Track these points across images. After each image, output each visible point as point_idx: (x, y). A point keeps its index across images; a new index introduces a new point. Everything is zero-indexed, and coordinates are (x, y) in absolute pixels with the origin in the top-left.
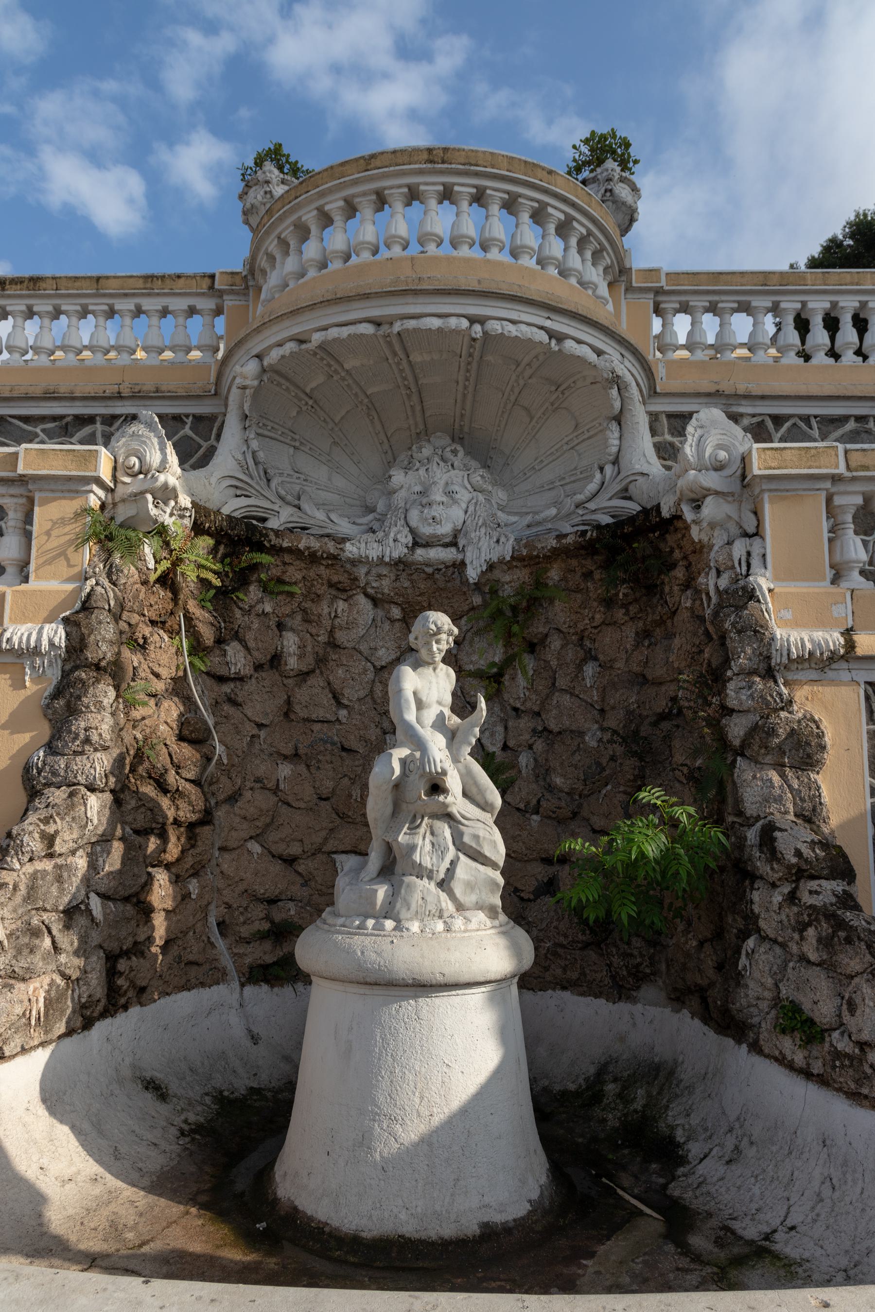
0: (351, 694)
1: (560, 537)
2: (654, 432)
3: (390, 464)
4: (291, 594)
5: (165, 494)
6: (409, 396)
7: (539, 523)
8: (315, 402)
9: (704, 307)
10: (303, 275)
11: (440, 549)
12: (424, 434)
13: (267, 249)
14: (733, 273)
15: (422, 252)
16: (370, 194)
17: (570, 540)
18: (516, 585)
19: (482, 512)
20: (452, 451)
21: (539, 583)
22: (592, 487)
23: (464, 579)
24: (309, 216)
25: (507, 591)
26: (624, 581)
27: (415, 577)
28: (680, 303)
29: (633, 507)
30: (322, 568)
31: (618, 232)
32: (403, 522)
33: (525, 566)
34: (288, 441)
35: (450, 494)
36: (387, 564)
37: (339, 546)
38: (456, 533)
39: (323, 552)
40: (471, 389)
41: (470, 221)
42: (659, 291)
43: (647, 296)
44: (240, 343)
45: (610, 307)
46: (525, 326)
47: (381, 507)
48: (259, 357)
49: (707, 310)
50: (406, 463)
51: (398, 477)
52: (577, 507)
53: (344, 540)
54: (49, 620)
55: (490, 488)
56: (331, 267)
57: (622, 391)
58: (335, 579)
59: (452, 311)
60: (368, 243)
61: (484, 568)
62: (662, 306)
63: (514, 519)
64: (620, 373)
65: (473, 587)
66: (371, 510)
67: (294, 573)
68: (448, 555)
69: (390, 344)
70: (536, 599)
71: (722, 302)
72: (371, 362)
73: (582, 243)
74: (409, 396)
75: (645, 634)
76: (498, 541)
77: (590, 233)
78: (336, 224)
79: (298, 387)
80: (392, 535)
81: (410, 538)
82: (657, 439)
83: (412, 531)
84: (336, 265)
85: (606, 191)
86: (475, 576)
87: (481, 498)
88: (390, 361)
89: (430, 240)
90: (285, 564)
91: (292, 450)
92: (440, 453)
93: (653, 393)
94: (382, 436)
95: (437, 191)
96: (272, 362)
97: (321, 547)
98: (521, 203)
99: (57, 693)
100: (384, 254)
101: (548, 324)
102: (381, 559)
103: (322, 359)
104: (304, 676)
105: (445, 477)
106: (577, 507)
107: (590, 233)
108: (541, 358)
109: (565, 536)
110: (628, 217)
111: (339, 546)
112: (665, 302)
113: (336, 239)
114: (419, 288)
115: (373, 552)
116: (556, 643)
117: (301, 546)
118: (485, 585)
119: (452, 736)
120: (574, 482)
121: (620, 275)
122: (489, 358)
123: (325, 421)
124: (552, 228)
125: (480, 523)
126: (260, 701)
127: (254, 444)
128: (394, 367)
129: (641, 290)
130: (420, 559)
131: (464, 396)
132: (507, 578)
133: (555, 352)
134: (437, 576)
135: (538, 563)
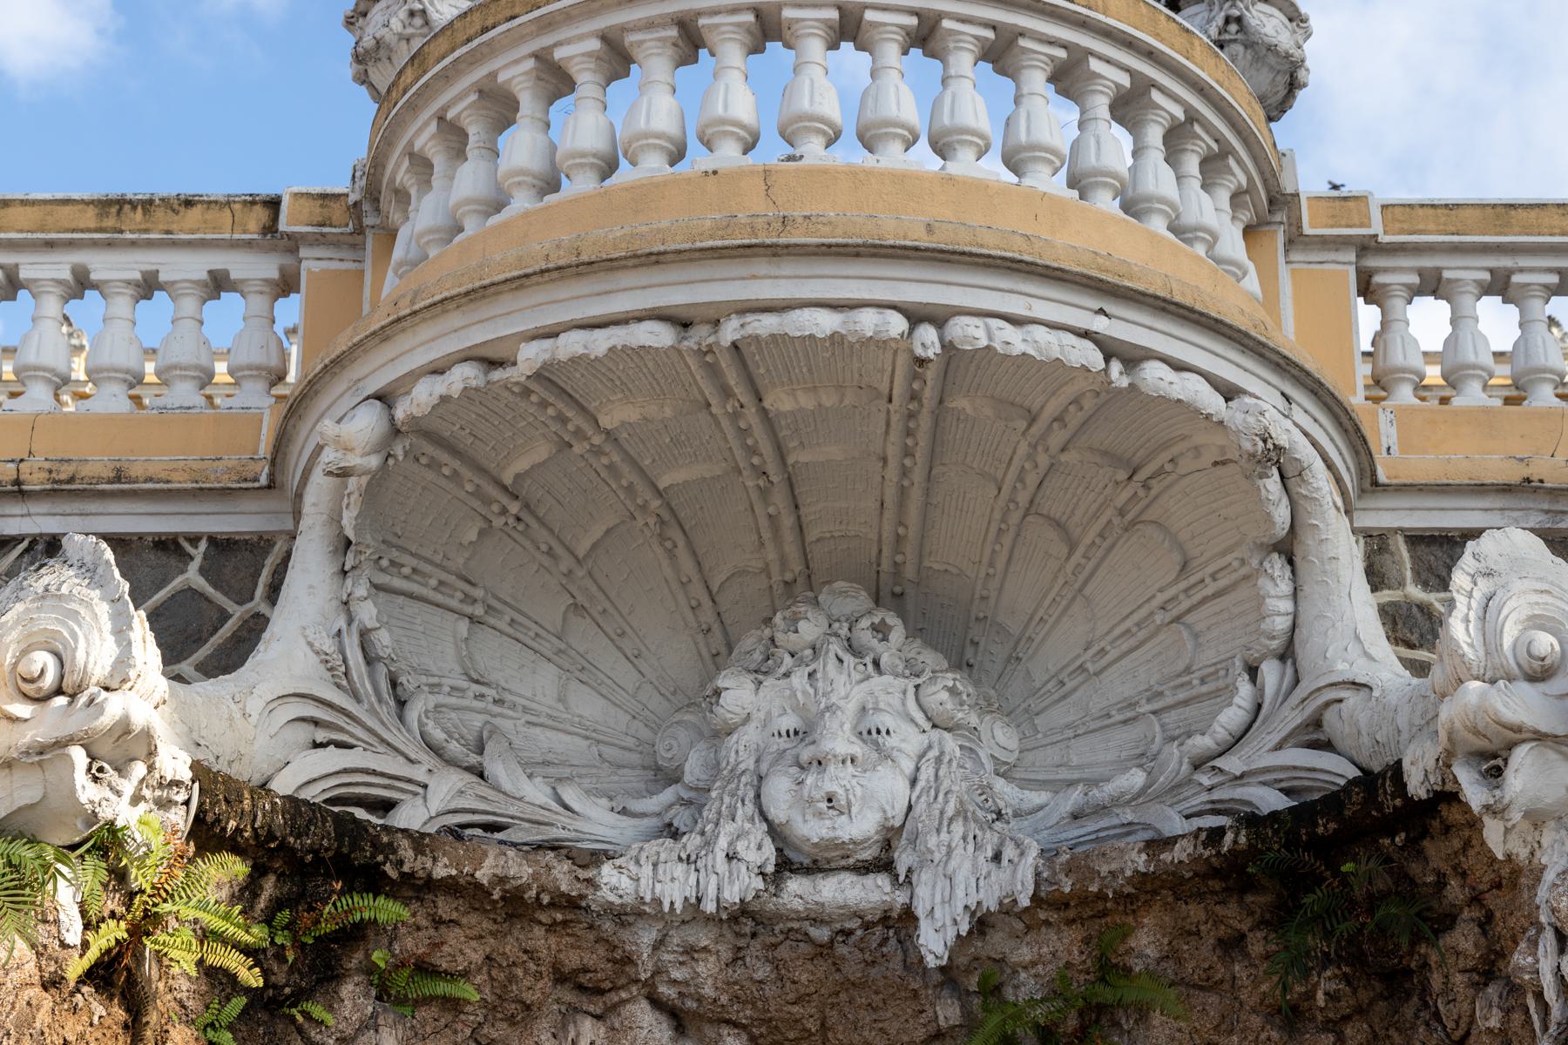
1: (1158, 844)
2: (1376, 578)
3: (718, 661)
4: (453, 1005)
6: (764, 493)
7: (1101, 809)
8: (527, 506)
9: (1478, 283)
10: (498, 206)
11: (848, 878)
12: (803, 585)
13: (411, 143)
14: (1542, 206)
15: (791, 158)
16: (664, 26)
17: (1181, 852)
18: (1048, 970)
19: (956, 783)
20: (875, 628)
21: (1108, 968)
22: (1232, 717)
23: (912, 958)
24: (516, 72)
26: (1326, 961)
27: (783, 952)
28: (1421, 272)
29: (1337, 769)
30: (539, 931)
31: (1261, 113)
32: (750, 808)
33: (1070, 922)
34: (454, 603)
35: (871, 735)
36: (709, 919)
37: (583, 874)
38: (889, 838)
39: (542, 889)
40: (918, 475)
41: (905, 89)
42: (1367, 246)
43: (1341, 257)
44: (336, 365)
45: (1252, 283)
47: (693, 769)
48: (384, 398)
49: (1487, 290)
50: (758, 656)
51: (738, 693)
52: (1197, 766)
53: (596, 858)
55: (974, 720)
56: (569, 189)
57: (1291, 483)
58: (572, 960)
59: (866, 296)
60: (659, 136)
61: (964, 928)
62: (1378, 279)
63: (1037, 798)
64: (1283, 441)
65: (938, 977)
66: (668, 776)
67: (463, 947)
68: (870, 893)
69: (713, 371)
70: (1101, 1009)
71: (1521, 270)
72: (668, 412)
73: (1175, 139)
74: (764, 493)
76: (997, 857)
77: (1192, 117)
78: (582, 91)
79: (481, 470)
80: (723, 843)
81: (769, 851)
82: (1387, 596)
83: (774, 831)
84: (580, 185)
85: (1228, 20)
86: (939, 949)
87: (951, 744)
88: (714, 410)
89: (809, 130)
90: (438, 922)
91: (463, 626)
92: (844, 632)
93: (1371, 484)
94: (698, 590)
95: (825, 22)
96: (417, 412)
97: (535, 877)
98: (1025, 50)
100: (698, 160)
101: (1100, 325)
102: (694, 906)
103: (544, 404)
105: (858, 694)
106: (1197, 766)
107: (1192, 117)
108: (1089, 404)
109: (1170, 842)
110: (1283, 79)
111: (583, 874)
112: (1386, 270)
113: (583, 124)
114: (783, 240)
115: (675, 888)
117: (483, 875)
118: (968, 971)
120: (1186, 703)
121: (1270, 210)
122: (960, 403)
123: (550, 552)
124: (1101, 105)
125: (950, 811)
127: (367, 613)
128: (725, 423)
129: (1325, 243)
130: (797, 905)
131: (903, 492)
132: (1025, 953)
133: (1120, 391)
134: (842, 950)
135: (1104, 913)
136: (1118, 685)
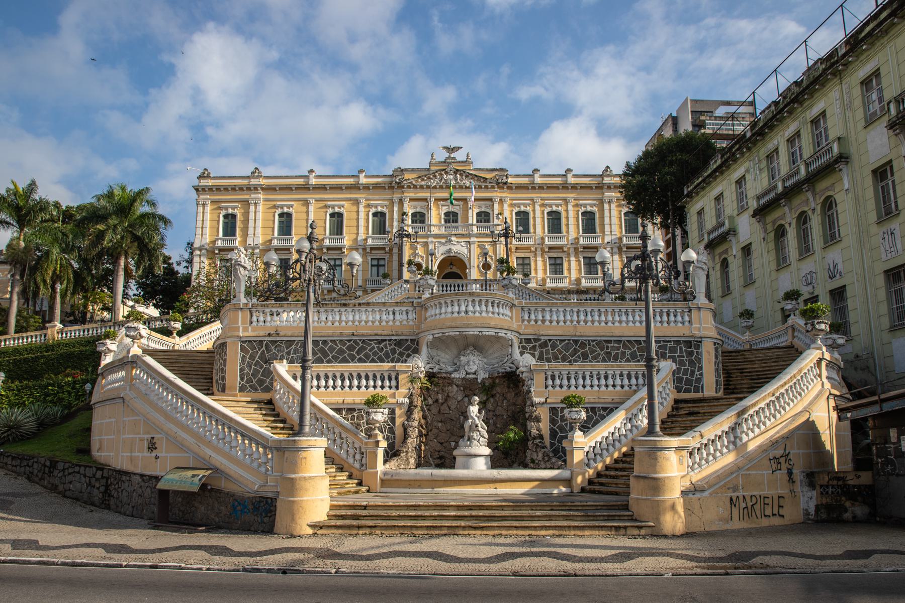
0: (453, 407)
5: (422, 372)
54: (405, 397)
104: (442, 404)
126: (434, 410)
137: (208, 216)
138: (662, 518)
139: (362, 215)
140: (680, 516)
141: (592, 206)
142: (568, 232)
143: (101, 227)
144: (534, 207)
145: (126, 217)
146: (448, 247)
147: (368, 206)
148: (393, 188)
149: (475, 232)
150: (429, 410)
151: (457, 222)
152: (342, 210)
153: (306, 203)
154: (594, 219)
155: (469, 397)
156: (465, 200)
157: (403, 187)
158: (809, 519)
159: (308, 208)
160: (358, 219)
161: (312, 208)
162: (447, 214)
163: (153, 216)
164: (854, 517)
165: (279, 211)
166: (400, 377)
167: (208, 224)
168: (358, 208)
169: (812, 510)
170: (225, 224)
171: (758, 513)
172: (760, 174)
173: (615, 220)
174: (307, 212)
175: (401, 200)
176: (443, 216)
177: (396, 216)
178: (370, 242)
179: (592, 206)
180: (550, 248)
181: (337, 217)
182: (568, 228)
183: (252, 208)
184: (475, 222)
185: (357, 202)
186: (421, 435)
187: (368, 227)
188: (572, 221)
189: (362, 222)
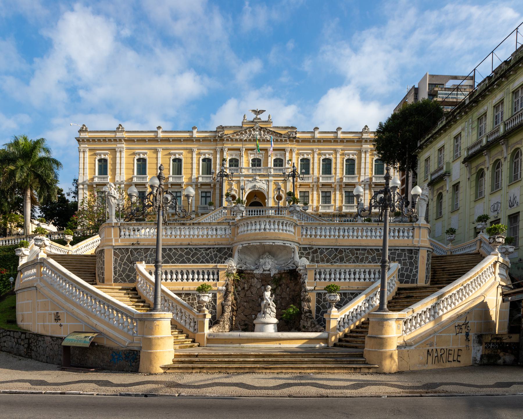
0: (254, 293)
5: (234, 270)
21: (281, 277)
25: (277, 278)
46: (280, 243)
51: (261, 260)
67: (246, 276)
68: (268, 272)
75: (295, 284)
99: (225, 295)
104: (247, 290)
115: (258, 272)
116: (283, 285)
119: (270, 299)
126: (242, 294)
136: (283, 258)
137: (87, 160)
138: (383, 363)
139: (195, 160)
140: (395, 361)
141: (353, 154)
142: (336, 174)
143: (12, 167)
144: (314, 155)
145: (29, 160)
146: (253, 184)
147: (199, 154)
148: (216, 140)
149: (272, 173)
150: (238, 294)
151: (260, 166)
152: (181, 157)
153: (156, 151)
154: (354, 164)
155: (265, 286)
156: (266, 150)
157: (223, 140)
158: (476, 364)
159: (157, 155)
160: (192, 163)
161: (160, 155)
162: (253, 160)
163: (48, 159)
164: (505, 362)
165: (137, 157)
166: (220, 273)
167: (87, 166)
168: (192, 155)
169: (478, 358)
170: (100, 166)
171: (444, 359)
172: (472, 131)
173: (368, 165)
174: (157, 158)
175: (222, 149)
176: (251, 162)
177: (218, 161)
178: (200, 180)
179: (353, 154)
180: (323, 185)
181: (178, 162)
182: (336, 171)
183: (118, 155)
184: (272, 166)
185: (191, 151)
186: (233, 310)
187: (199, 169)
188: (339, 166)
189: (195, 166)
